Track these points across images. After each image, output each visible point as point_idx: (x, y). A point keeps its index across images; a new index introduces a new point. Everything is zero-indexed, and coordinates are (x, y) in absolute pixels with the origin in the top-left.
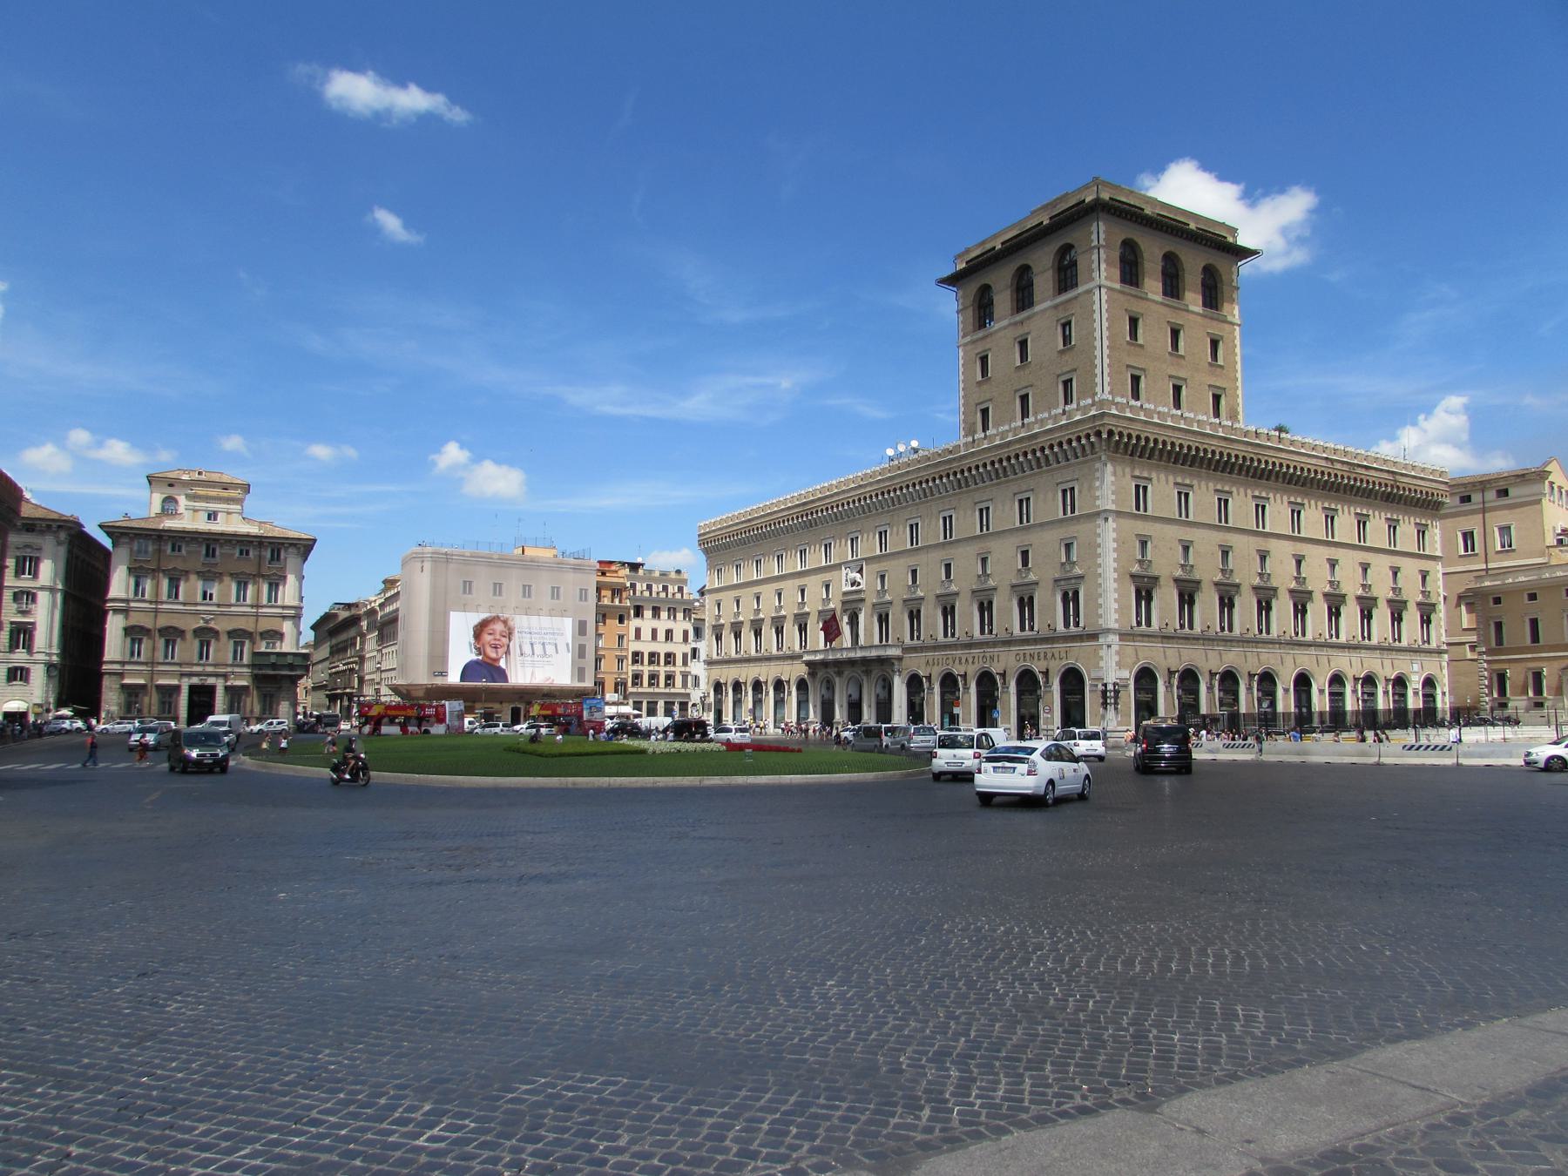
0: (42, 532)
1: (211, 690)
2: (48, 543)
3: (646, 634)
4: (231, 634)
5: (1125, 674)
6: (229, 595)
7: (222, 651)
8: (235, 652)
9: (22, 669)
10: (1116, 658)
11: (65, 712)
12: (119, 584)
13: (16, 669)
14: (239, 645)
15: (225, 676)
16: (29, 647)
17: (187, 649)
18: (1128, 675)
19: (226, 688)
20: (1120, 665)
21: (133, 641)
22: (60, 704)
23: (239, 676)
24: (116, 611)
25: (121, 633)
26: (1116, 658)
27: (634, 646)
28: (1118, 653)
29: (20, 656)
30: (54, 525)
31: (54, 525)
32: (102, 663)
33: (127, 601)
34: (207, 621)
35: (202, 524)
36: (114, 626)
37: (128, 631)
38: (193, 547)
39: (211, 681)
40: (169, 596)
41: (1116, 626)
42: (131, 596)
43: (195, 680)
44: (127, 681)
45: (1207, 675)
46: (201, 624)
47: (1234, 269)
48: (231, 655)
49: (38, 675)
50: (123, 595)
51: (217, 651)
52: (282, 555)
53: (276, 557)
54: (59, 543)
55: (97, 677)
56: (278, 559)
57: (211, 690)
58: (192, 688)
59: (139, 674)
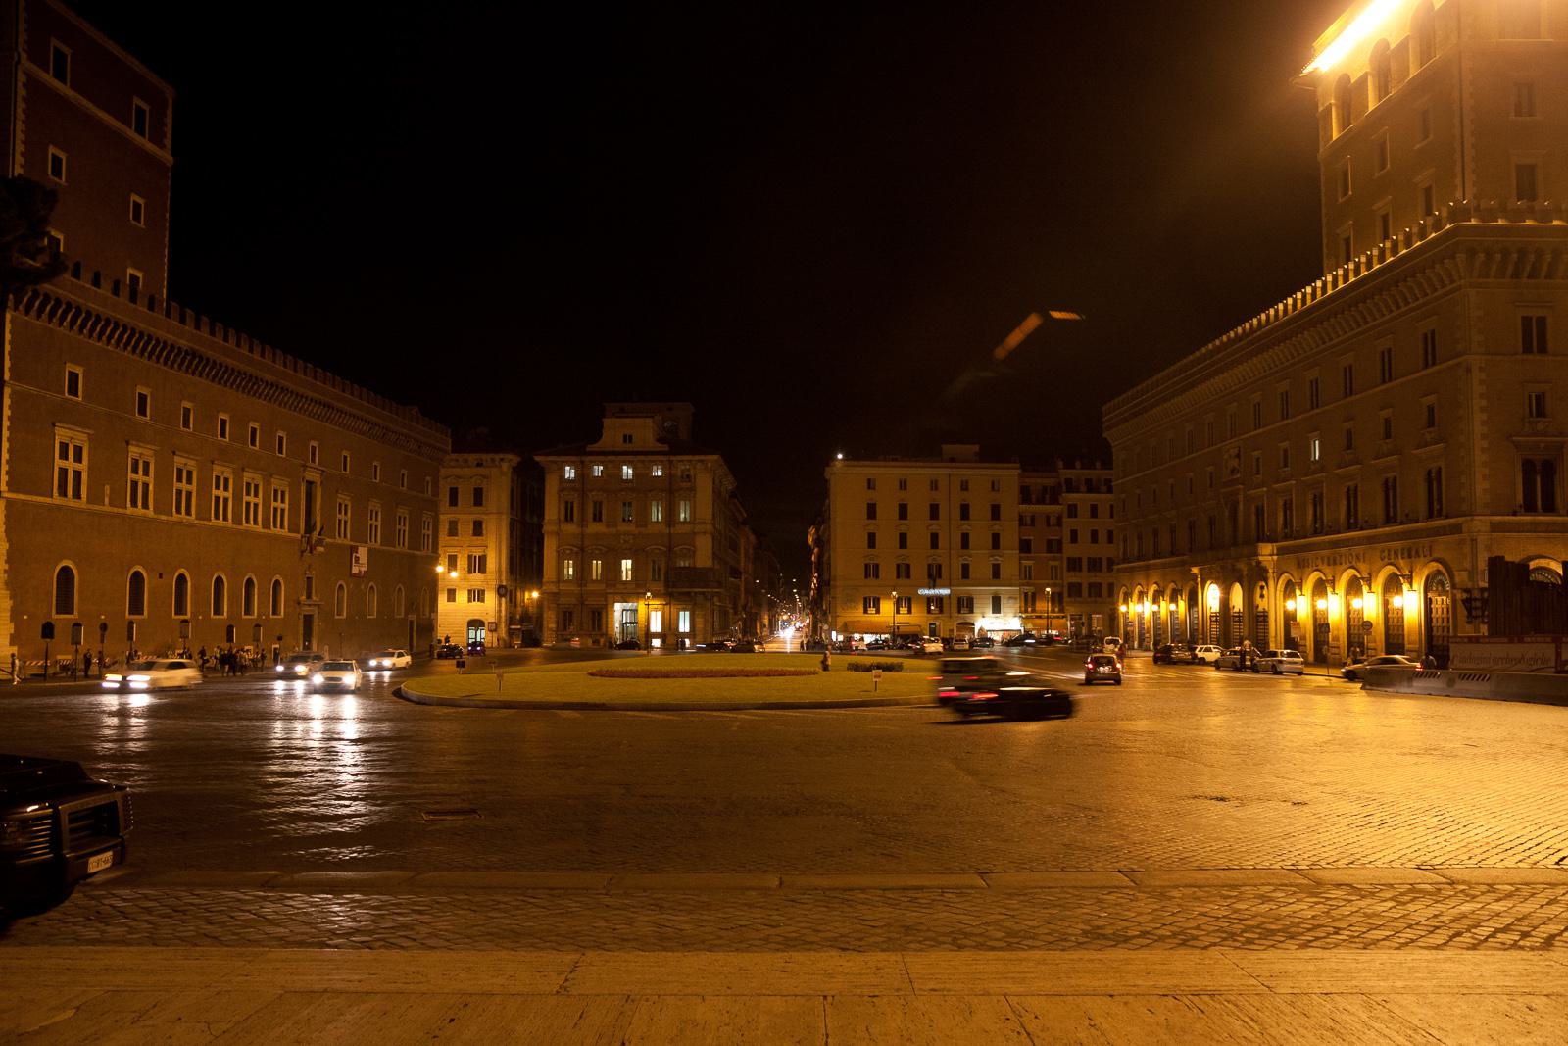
3: (1084, 536)
27: (1070, 551)
35: (621, 446)
42: (563, 518)
44: (562, 600)
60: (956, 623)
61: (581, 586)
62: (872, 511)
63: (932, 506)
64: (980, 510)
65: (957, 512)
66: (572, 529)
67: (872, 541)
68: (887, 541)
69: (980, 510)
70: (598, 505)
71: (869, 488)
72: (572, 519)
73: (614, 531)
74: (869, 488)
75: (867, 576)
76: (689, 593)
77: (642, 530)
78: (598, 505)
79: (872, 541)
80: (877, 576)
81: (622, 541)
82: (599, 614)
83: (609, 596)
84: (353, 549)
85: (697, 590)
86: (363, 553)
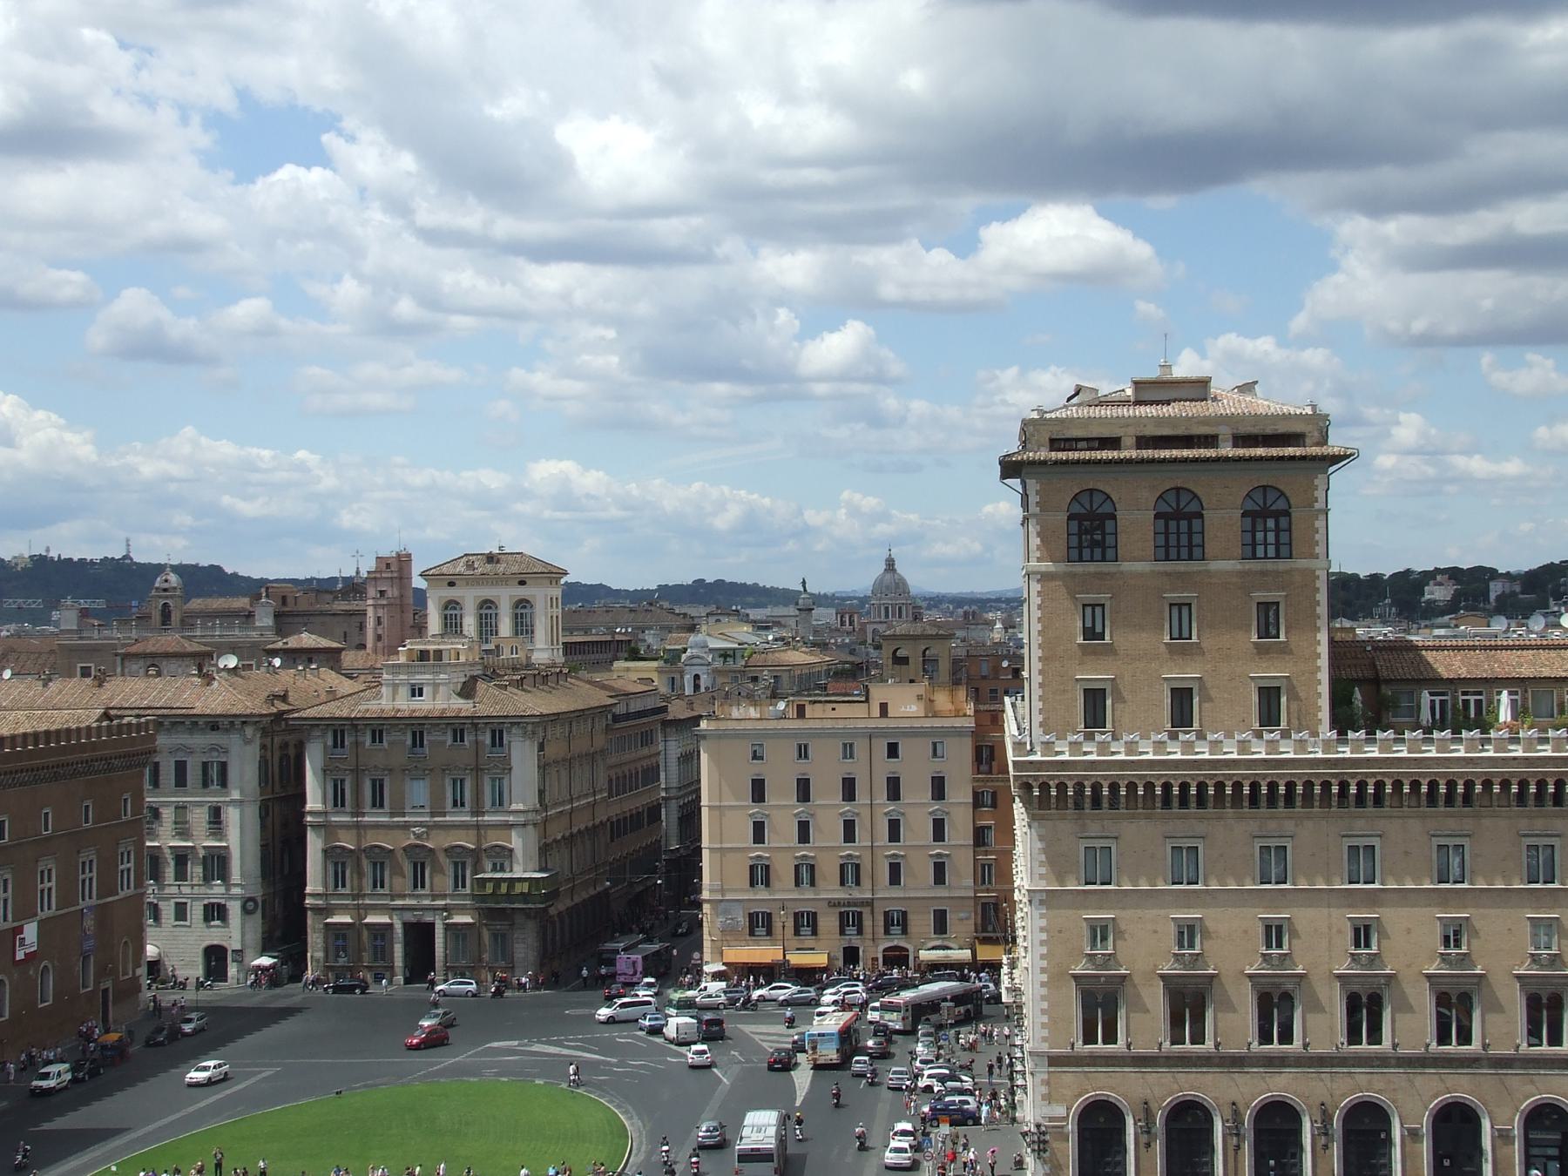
0: (227, 730)
2: (233, 741)
4: (449, 851)
5: (1060, 1111)
6: (444, 799)
8: (456, 877)
9: (219, 905)
10: (1044, 1090)
11: (266, 961)
13: (213, 905)
14: (459, 867)
15: (445, 908)
16: (224, 875)
18: (1066, 1113)
19: (448, 927)
20: (1048, 1098)
21: (336, 864)
22: (264, 951)
23: (462, 909)
24: (315, 826)
25: (320, 855)
26: (1044, 1090)
28: (1047, 1083)
29: (218, 888)
30: (237, 722)
31: (237, 722)
32: (303, 896)
33: (326, 813)
34: (418, 837)
35: (404, 704)
36: (314, 845)
37: (327, 853)
38: (395, 736)
39: (428, 918)
40: (374, 805)
41: (1045, 1048)
43: (410, 917)
45: (1228, 1114)
46: (412, 840)
47: (1319, 481)
48: (451, 882)
49: (234, 909)
50: (319, 806)
53: (498, 739)
54: (247, 742)
55: (302, 911)
56: (501, 745)
57: (432, 925)
58: (407, 926)
59: (344, 909)
60: (881, 948)
62: (759, 791)
68: (783, 833)
71: (755, 757)
72: (343, 805)
74: (755, 757)
80: (768, 885)
82: (383, 937)
84: (20, 930)
86: (31, 932)
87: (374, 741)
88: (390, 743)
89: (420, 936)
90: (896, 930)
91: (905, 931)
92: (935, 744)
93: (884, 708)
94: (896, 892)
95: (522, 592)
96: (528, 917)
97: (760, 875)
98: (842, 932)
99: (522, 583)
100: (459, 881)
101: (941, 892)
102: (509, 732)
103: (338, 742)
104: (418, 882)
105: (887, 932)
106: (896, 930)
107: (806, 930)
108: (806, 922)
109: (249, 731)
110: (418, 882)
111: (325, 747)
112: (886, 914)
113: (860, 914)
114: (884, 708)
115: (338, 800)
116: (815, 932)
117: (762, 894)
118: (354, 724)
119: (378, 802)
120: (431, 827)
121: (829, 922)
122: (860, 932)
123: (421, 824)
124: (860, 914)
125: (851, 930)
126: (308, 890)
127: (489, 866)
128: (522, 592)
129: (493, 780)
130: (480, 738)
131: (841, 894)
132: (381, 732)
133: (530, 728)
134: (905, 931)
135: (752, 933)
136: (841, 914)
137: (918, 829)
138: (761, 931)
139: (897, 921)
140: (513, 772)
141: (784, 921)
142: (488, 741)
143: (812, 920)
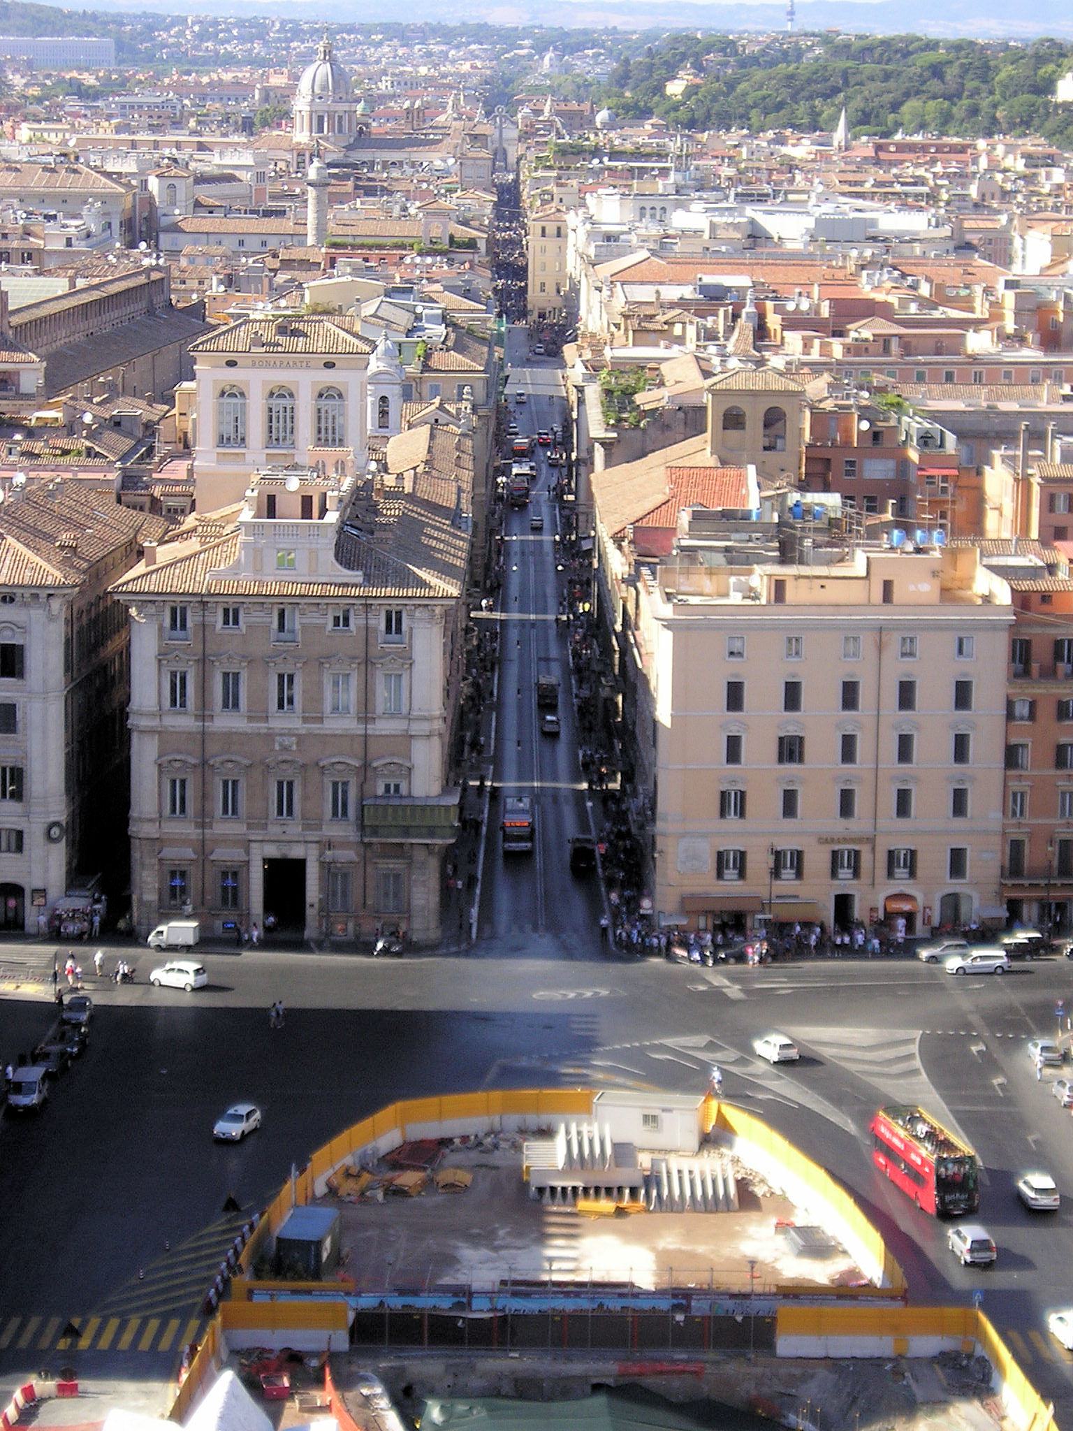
0: (25, 605)
1: (300, 864)
2: (36, 615)
6: (320, 700)
7: (315, 798)
12: (146, 689)
17: (258, 796)
23: (344, 845)
32: (124, 820)
39: (296, 852)
40: (226, 705)
43: (273, 851)
44: (168, 852)
51: (305, 798)
52: (404, 627)
54: (51, 618)
56: (399, 631)
57: (300, 864)
61: (203, 826)
63: (845, 684)
64: (935, 695)
65: (891, 695)
66: (185, 722)
67: (733, 749)
69: (935, 695)
70: (230, 681)
72: (183, 705)
73: (262, 726)
75: (723, 813)
76: (402, 845)
77: (314, 727)
78: (230, 681)
79: (733, 749)
80: (742, 814)
81: (277, 747)
82: (235, 874)
83: (253, 845)
85: (414, 841)
87: (226, 622)
88: (249, 627)
89: (285, 878)
90: (901, 872)
91: (912, 874)
92: (961, 641)
93: (888, 585)
94: (903, 823)
95: (329, 377)
96: (431, 853)
97: (732, 803)
98: (834, 874)
99: (330, 365)
100: (340, 810)
101: (959, 823)
102: (411, 616)
103: (178, 619)
104: (285, 806)
105: (890, 874)
106: (901, 872)
107: (788, 873)
108: (787, 862)
109: (56, 604)
110: (285, 806)
111: (161, 628)
112: (891, 853)
113: (857, 853)
114: (888, 585)
115: (177, 695)
116: (799, 874)
117: (732, 821)
118: (203, 601)
119: (230, 701)
120: (301, 739)
121: (817, 860)
122: (856, 874)
123: (290, 733)
124: (857, 853)
125: (845, 873)
126: (134, 813)
127: (381, 791)
128: (329, 377)
129: (388, 676)
130: (372, 622)
131: (838, 826)
132: (236, 612)
133: (438, 610)
134: (912, 874)
135: (720, 875)
136: (835, 853)
137: (933, 748)
138: (730, 873)
139: (904, 862)
140: (416, 668)
141: (759, 863)
142: (383, 626)
143: (798, 856)
